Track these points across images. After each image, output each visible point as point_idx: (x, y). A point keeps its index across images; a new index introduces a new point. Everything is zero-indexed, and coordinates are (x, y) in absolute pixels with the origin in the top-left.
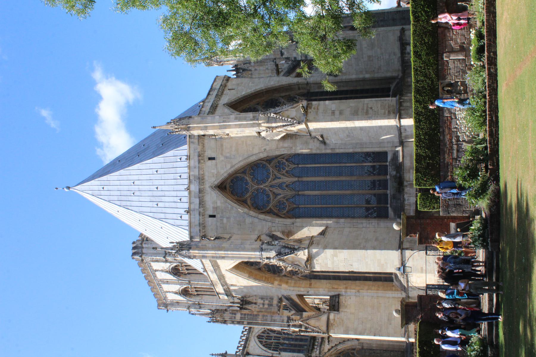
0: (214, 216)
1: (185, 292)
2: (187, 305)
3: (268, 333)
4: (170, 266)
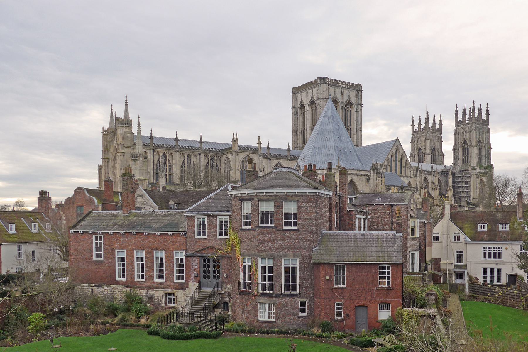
1: (302, 106)
2: (296, 106)
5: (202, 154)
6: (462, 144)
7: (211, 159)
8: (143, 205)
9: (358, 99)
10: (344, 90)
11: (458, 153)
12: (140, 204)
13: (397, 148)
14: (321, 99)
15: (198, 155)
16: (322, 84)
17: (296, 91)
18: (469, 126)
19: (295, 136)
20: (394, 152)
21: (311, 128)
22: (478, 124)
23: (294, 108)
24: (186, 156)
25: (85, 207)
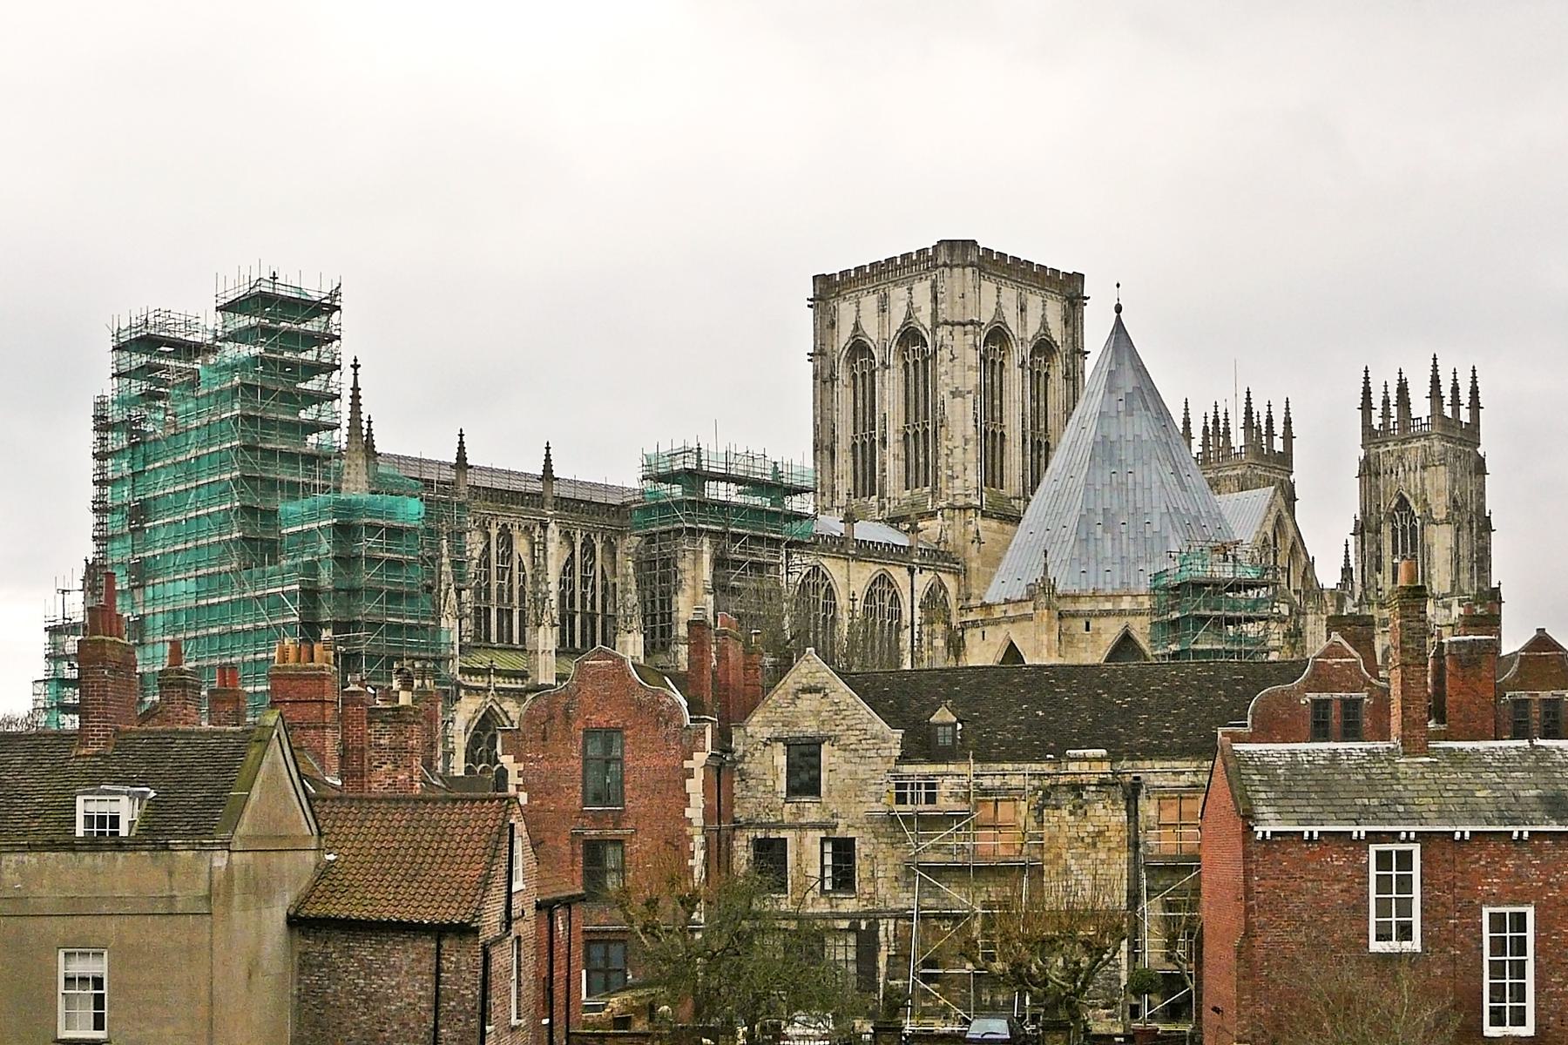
0: (1088, 629)
1: (859, 348)
2: (827, 349)
3: (823, 585)
4: (922, 325)
5: (552, 525)
6: (1390, 511)
7: (582, 545)
8: (827, 728)
9: (1070, 330)
10: (1029, 295)
11: (1375, 546)
12: (814, 723)
13: (1279, 521)
14: (953, 324)
15: (538, 528)
16: (957, 266)
17: (827, 289)
18: (1418, 448)
19: (827, 459)
20: (1270, 534)
21: (901, 438)
22: (1449, 439)
23: (818, 354)
24: (494, 532)
25: (628, 732)
